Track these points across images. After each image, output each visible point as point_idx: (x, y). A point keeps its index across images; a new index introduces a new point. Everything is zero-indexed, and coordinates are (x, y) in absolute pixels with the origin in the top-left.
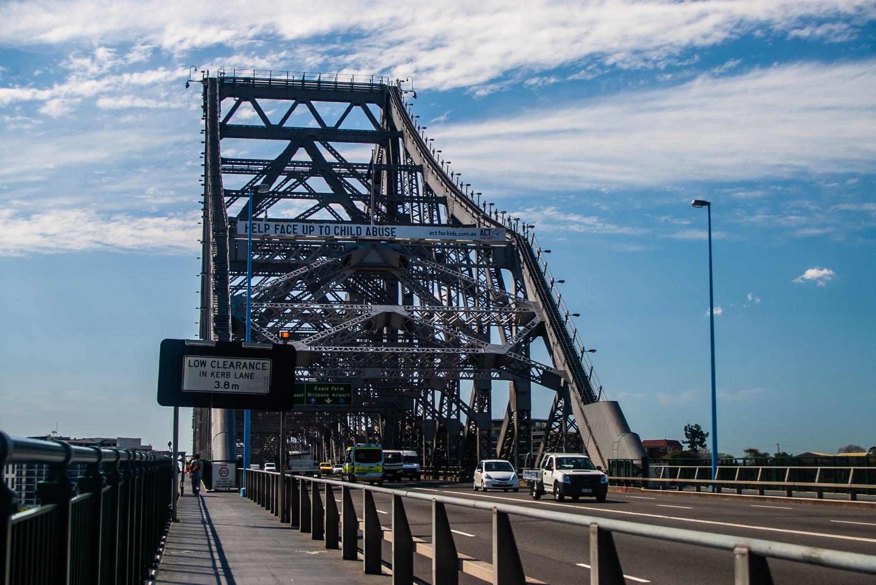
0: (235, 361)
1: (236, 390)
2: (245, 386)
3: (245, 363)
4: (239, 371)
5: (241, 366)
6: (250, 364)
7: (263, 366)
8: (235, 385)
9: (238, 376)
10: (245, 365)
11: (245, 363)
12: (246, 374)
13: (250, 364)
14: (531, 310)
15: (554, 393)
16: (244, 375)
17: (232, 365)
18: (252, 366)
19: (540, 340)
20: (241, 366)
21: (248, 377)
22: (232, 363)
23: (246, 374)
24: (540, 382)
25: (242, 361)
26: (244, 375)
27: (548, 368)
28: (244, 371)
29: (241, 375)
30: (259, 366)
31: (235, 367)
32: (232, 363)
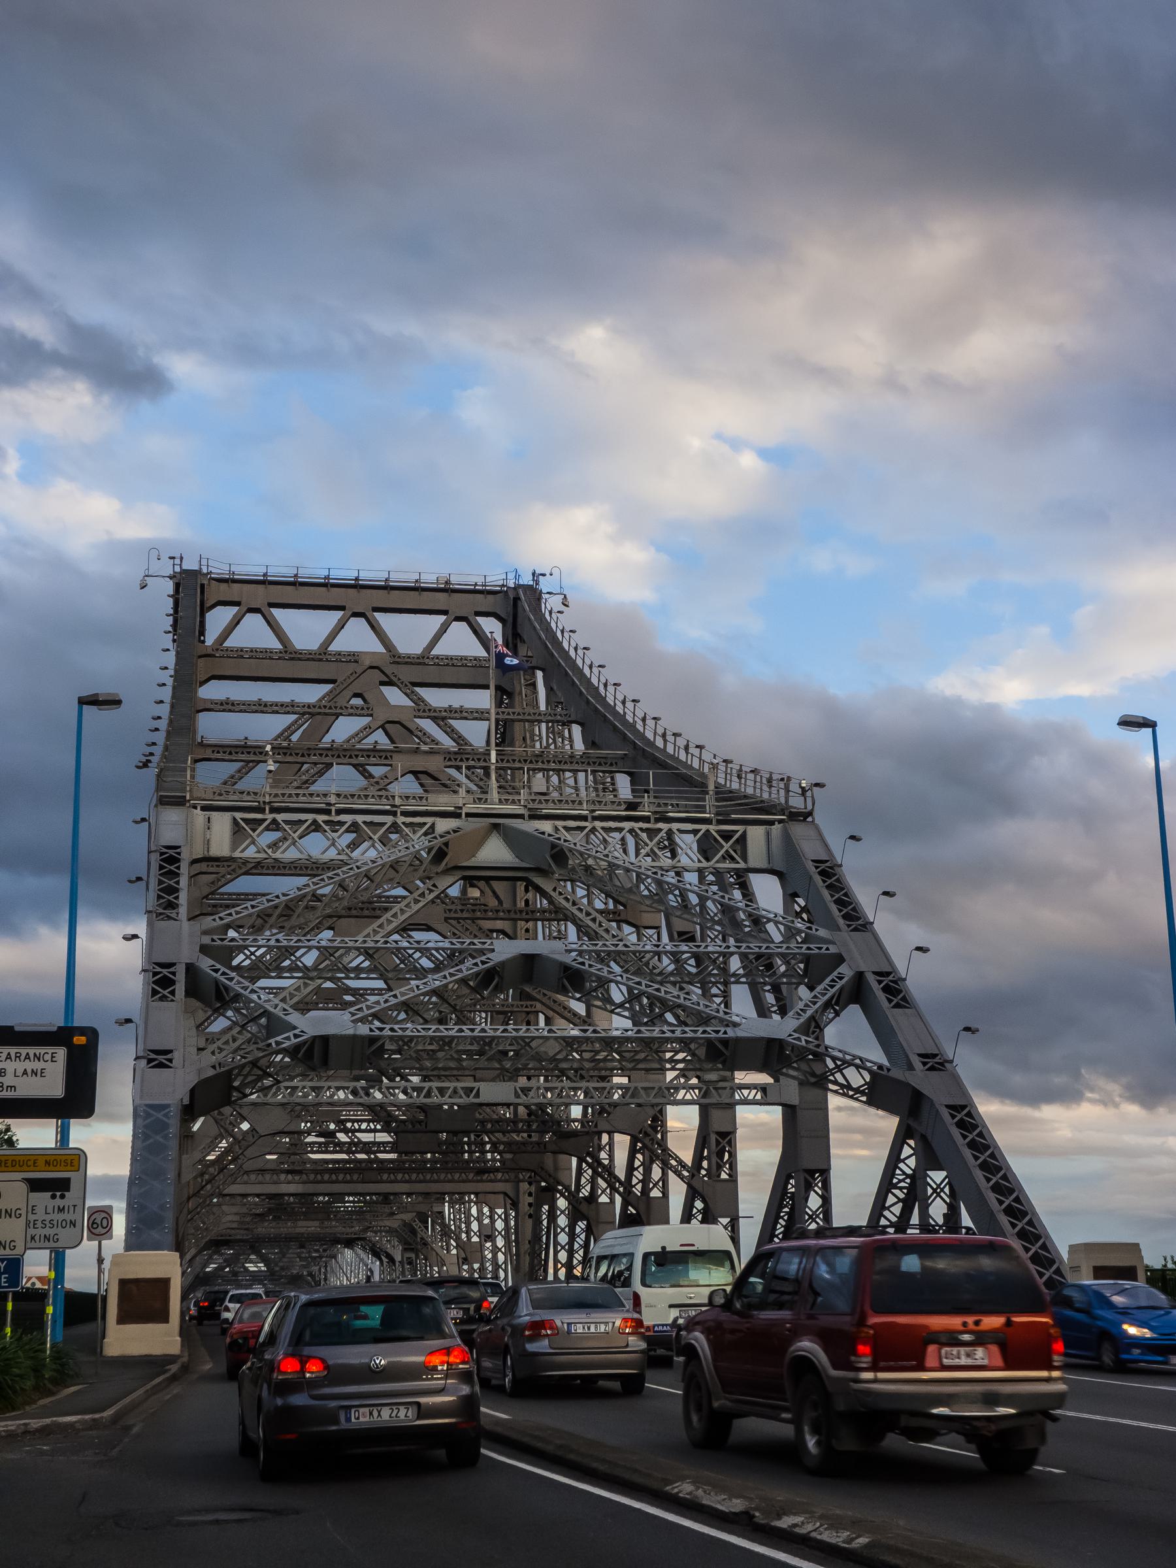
0: (13, 1051)
1: (12, 1093)
2: (29, 1088)
3: (28, 1054)
4: (20, 1066)
5: (23, 1057)
6: (35, 1054)
7: (52, 1057)
8: (11, 1087)
9: (20, 1072)
10: (27, 1057)
11: (28, 1054)
12: (33, 1070)
13: (35, 1054)
14: (833, 949)
15: (889, 1124)
16: (29, 1071)
17: (9, 1057)
18: (38, 1057)
19: (854, 1012)
20: (23, 1057)
21: (36, 1075)
22: (9, 1054)
23: (33, 1070)
24: (864, 1099)
25: (24, 1051)
26: (29, 1071)
27: (880, 1067)
28: (30, 1065)
29: (25, 1072)
30: (48, 1057)
31: (13, 1057)
32: (9, 1054)
